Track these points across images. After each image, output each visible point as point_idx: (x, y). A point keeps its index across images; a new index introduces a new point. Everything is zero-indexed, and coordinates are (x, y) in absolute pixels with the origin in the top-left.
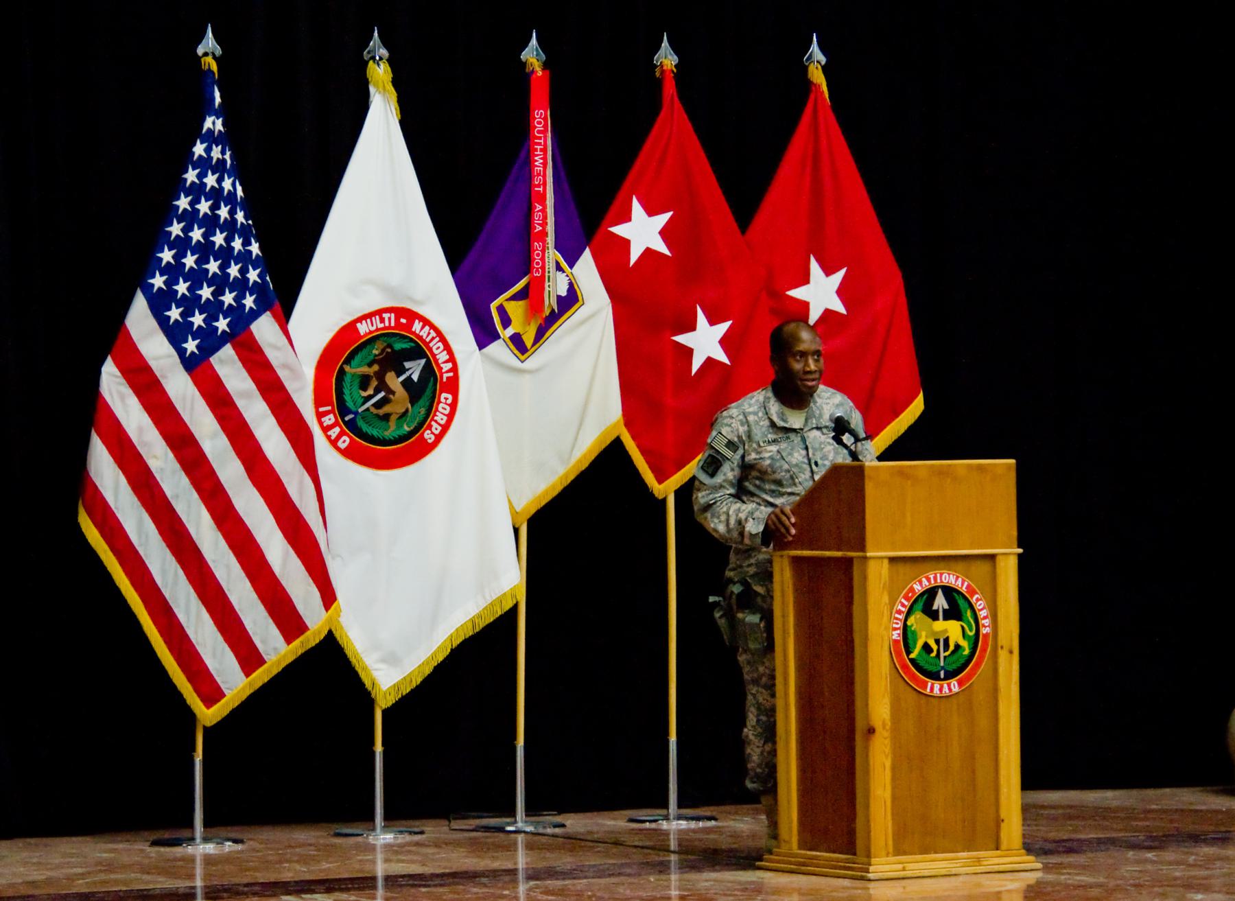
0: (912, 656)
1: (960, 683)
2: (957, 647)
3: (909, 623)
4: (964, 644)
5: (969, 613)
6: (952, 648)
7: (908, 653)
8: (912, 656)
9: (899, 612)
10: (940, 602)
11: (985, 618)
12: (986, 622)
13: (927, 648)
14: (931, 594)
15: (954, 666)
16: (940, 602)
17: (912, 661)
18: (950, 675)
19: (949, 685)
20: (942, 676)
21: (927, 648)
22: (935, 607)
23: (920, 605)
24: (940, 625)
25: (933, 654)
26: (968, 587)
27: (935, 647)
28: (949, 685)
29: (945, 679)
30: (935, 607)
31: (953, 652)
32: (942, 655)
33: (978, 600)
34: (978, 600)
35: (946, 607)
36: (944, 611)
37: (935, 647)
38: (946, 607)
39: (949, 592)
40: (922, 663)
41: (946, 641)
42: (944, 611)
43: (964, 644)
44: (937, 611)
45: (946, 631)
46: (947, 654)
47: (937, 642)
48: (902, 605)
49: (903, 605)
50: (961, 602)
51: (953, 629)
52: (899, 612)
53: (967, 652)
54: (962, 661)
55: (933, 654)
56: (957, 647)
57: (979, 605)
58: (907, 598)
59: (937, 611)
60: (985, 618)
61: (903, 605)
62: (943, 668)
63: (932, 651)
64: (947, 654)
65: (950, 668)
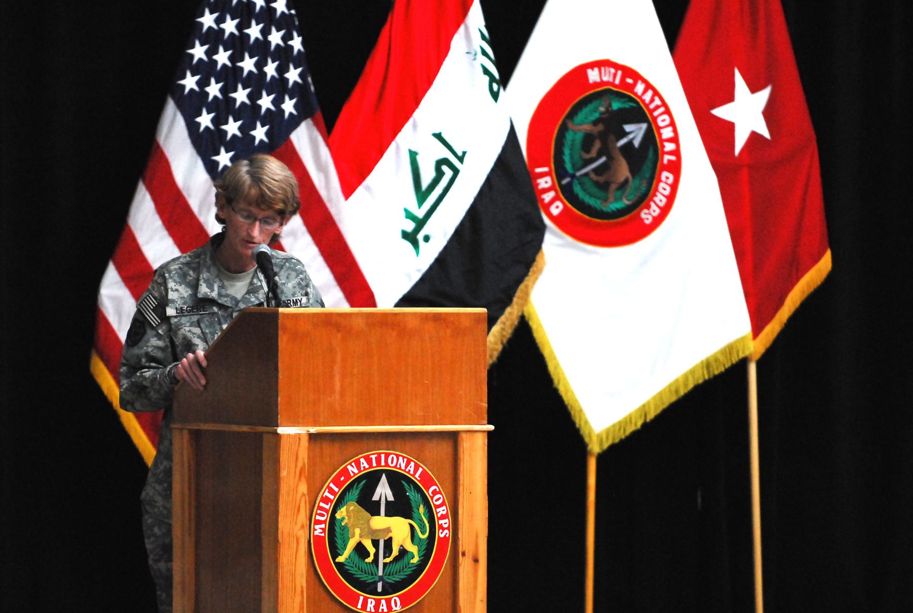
0: (340, 559)
1: (404, 601)
2: (403, 552)
3: (338, 516)
4: (413, 549)
5: (422, 509)
6: (395, 553)
7: (335, 555)
8: (340, 559)
9: (326, 500)
10: (383, 491)
11: (443, 517)
12: (445, 523)
13: (360, 550)
14: (372, 479)
15: (397, 578)
16: (383, 491)
17: (340, 566)
18: (390, 589)
19: (388, 602)
20: (380, 589)
21: (360, 550)
22: (376, 498)
23: (355, 493)
24: (380, 522)
25: (370, 560)
26: (424, 473)
27: (372, 550)
28: (388, 602)
29: (384, 592)
30: (376, 498)
31: (397, 559)
32: (381, 561)
33: (435, 493)
34: (435, 493)
35: (391, 498)
36: (388, 503)
37: (372, 550)
38: (391, 498)
39: (397, 480)
40: (353, 571)
41: (389, 543)
42: (388, 503)
43: (413, 549)
44: (378, 503)
45: (388, 530)
46: (388, 560)
47: (375, 543)
48: (330, 491)
49: (331, 491)
50: (411, 494)
51: (399, 529)
52: (326, 500)
53: (415, 560)
54: (408, 571)
55: (370, 560)
56: (403, 552)
57: (436, 500)
58: (336, 482)
59: (378, 503)
60: (443, 517)
61: (331, 491)
62: (381, 578)
63: (367, 554)
64: (388, 560)
65: (391, 580)
